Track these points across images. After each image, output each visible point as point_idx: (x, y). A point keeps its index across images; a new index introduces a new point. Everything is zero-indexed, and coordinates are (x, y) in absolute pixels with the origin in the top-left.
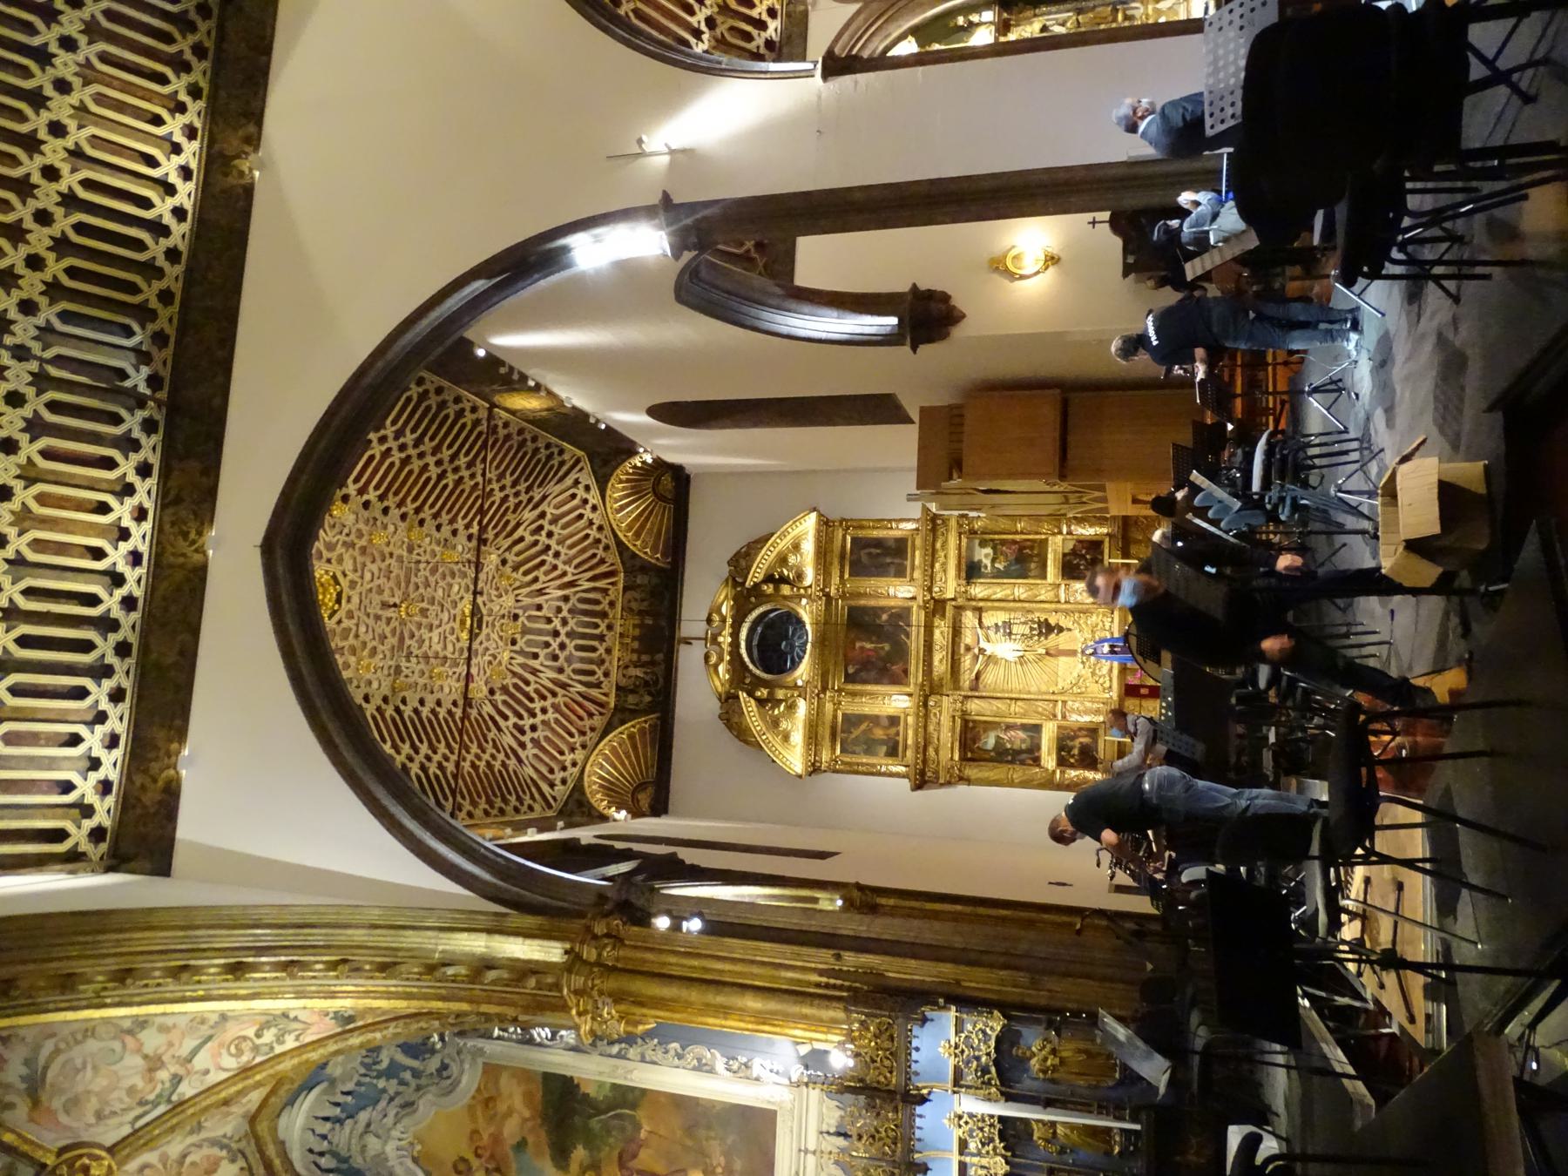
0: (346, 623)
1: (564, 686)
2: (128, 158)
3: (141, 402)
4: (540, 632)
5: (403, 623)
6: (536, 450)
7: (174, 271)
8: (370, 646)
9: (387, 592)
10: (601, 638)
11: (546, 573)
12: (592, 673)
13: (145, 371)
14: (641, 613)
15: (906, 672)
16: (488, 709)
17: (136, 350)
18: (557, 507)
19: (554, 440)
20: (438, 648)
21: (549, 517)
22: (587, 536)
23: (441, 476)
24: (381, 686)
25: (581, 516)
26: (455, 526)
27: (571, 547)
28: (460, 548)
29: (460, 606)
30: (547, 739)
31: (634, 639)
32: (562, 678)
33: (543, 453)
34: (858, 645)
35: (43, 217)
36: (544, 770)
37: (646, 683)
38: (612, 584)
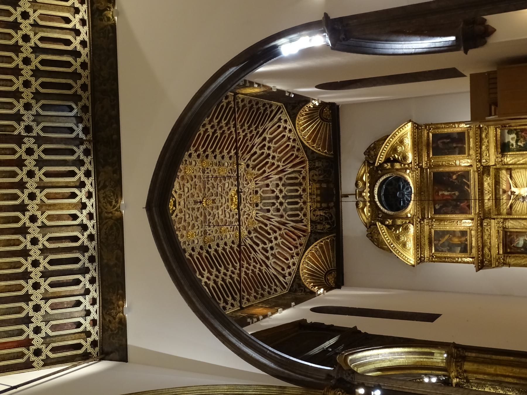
0: (180, 215)
1: (284, 224)
2: (57, 21)
3: (82, 142)
4: (269, 198)
5: (205, 209)
6: (258, 109)
7: (85, 73)
9: (196, 195)
10: (300, 196)
11: (269, 168)
12: (298, 215)
13: (81, 126)
14: (319, 182)
15: (469, 206)
16: (249, 241)
17: (75, 116)
18: (271, 134)
19: (266, 101)
20: (222, 217)
21: (268, 139)
22: (288, 145)
23: (214, 133)
24: (198, 241)
25: (284, 136)
26: (223, 154)
27: (280, 153)
28: (226, 164)
29: (230, 194)
30: (279, 252)
31: (317, 195)
32: (282, 220)
33: (262, 109)
34: (440, 193)
35: (27, 61)
36: (279, 269)
37: (326, 219)
38: (303, 168)
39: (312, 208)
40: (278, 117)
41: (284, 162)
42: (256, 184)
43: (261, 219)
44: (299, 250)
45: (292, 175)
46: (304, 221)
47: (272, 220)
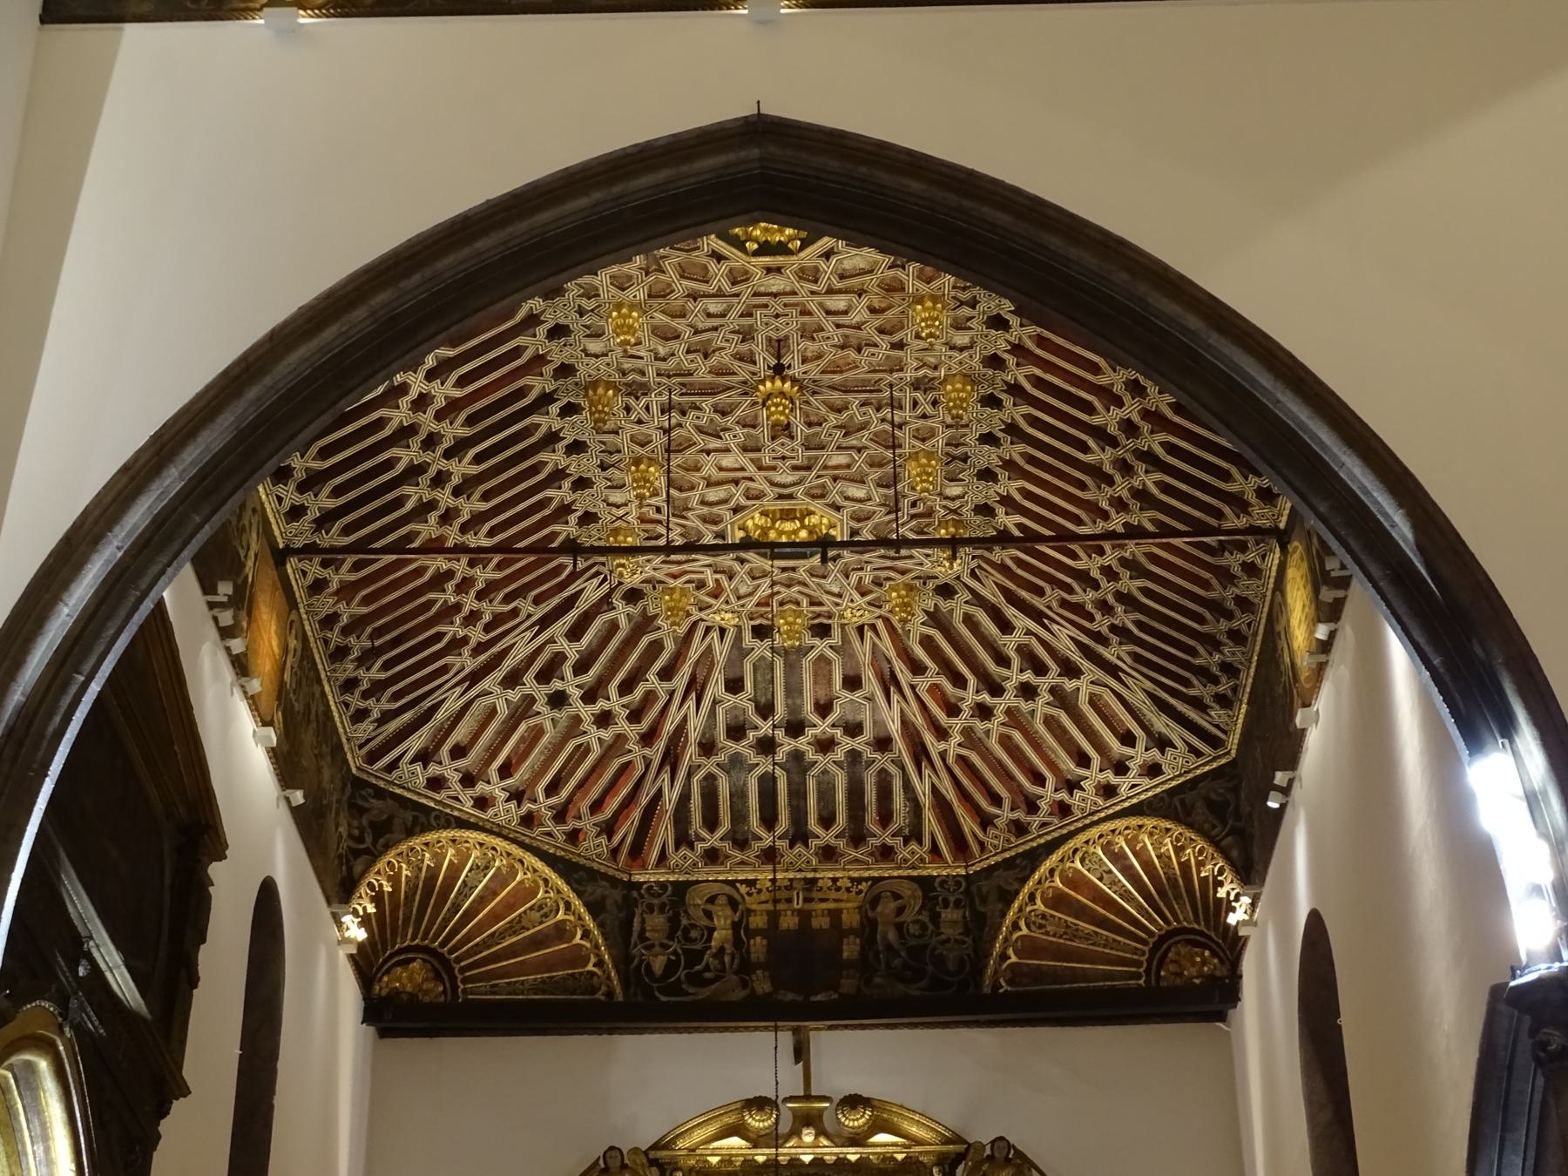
0: (719, 272)
1: (671, 759)
4: (793, 690)
5: (748, 389)
6: (1213, 643)
8: (679, 325)
9: (812, 347)
10: (800, 835)
11: (935, 689)
12: (711, 823)
14: (868, 927)
16: (592, 592)
18: (1094, 701)
19: (1248, 680)
20: (709, 469)
21: (1069, 685)
22: (1039, 780)
23: (1100, 433)
24: (595, 357)
25: (1083, 760)
26: (1003, 475)
27: (1005, 741)
28: (954, 490)
29: (815, 505)
30: (538, 732)
31: (805, 916)
32: (691, 753)
33: (1209, 660)
36: (460, 734)
37: (694, 957)
38: (935, 849)
39: (743, 889)
40: (1175, 732)
41: (961, 759)
42: (860, 629)
43: (694, 653)
44: (550, 826)
45: (899, 800)
46: (684, 851)
47: (691, 703)
